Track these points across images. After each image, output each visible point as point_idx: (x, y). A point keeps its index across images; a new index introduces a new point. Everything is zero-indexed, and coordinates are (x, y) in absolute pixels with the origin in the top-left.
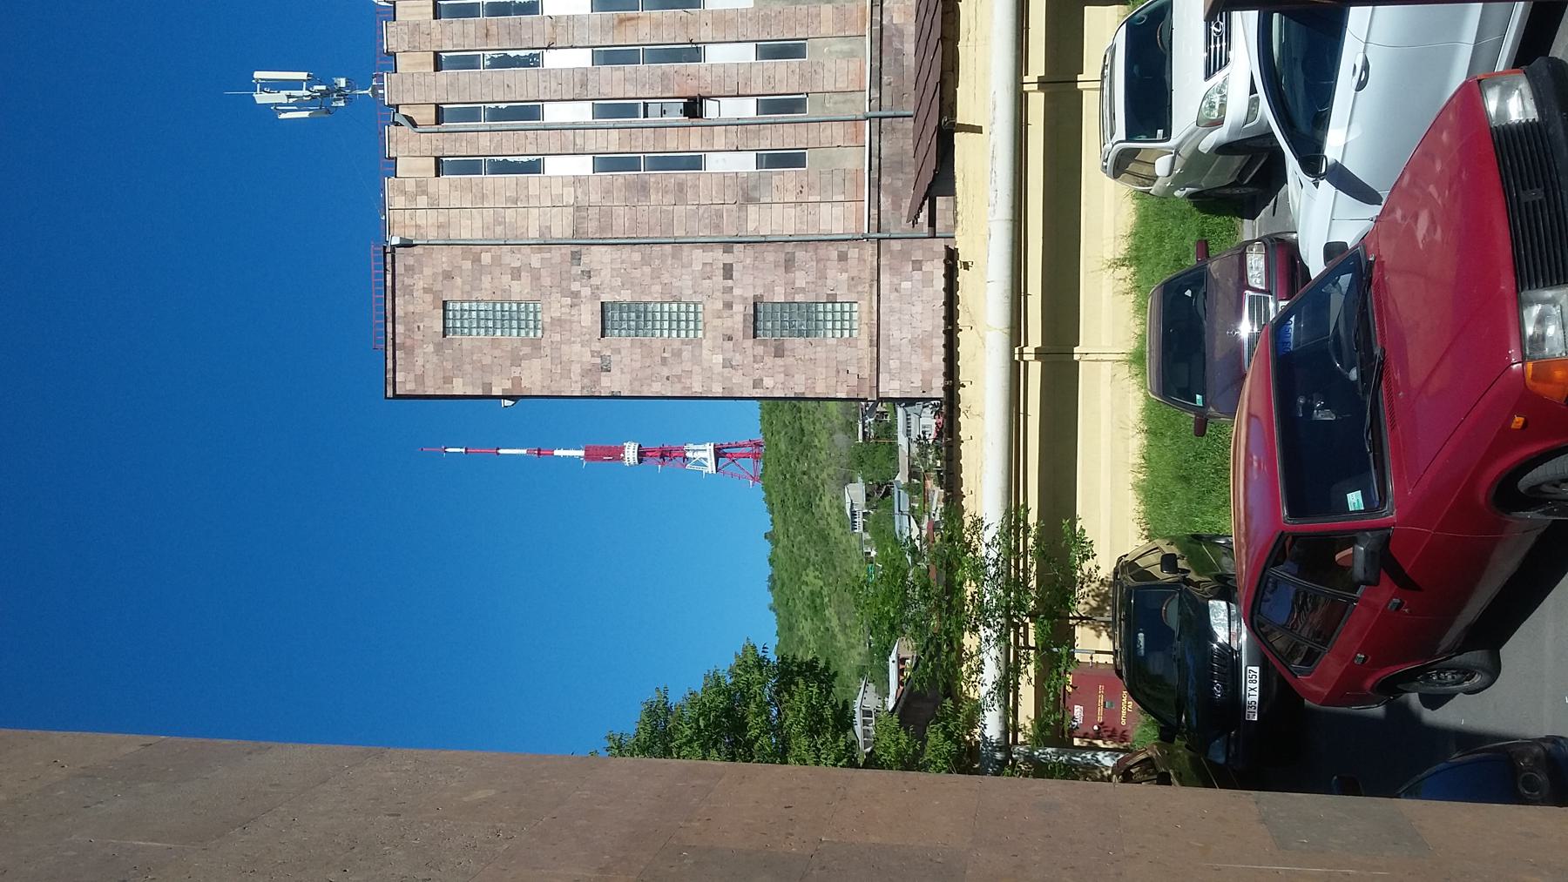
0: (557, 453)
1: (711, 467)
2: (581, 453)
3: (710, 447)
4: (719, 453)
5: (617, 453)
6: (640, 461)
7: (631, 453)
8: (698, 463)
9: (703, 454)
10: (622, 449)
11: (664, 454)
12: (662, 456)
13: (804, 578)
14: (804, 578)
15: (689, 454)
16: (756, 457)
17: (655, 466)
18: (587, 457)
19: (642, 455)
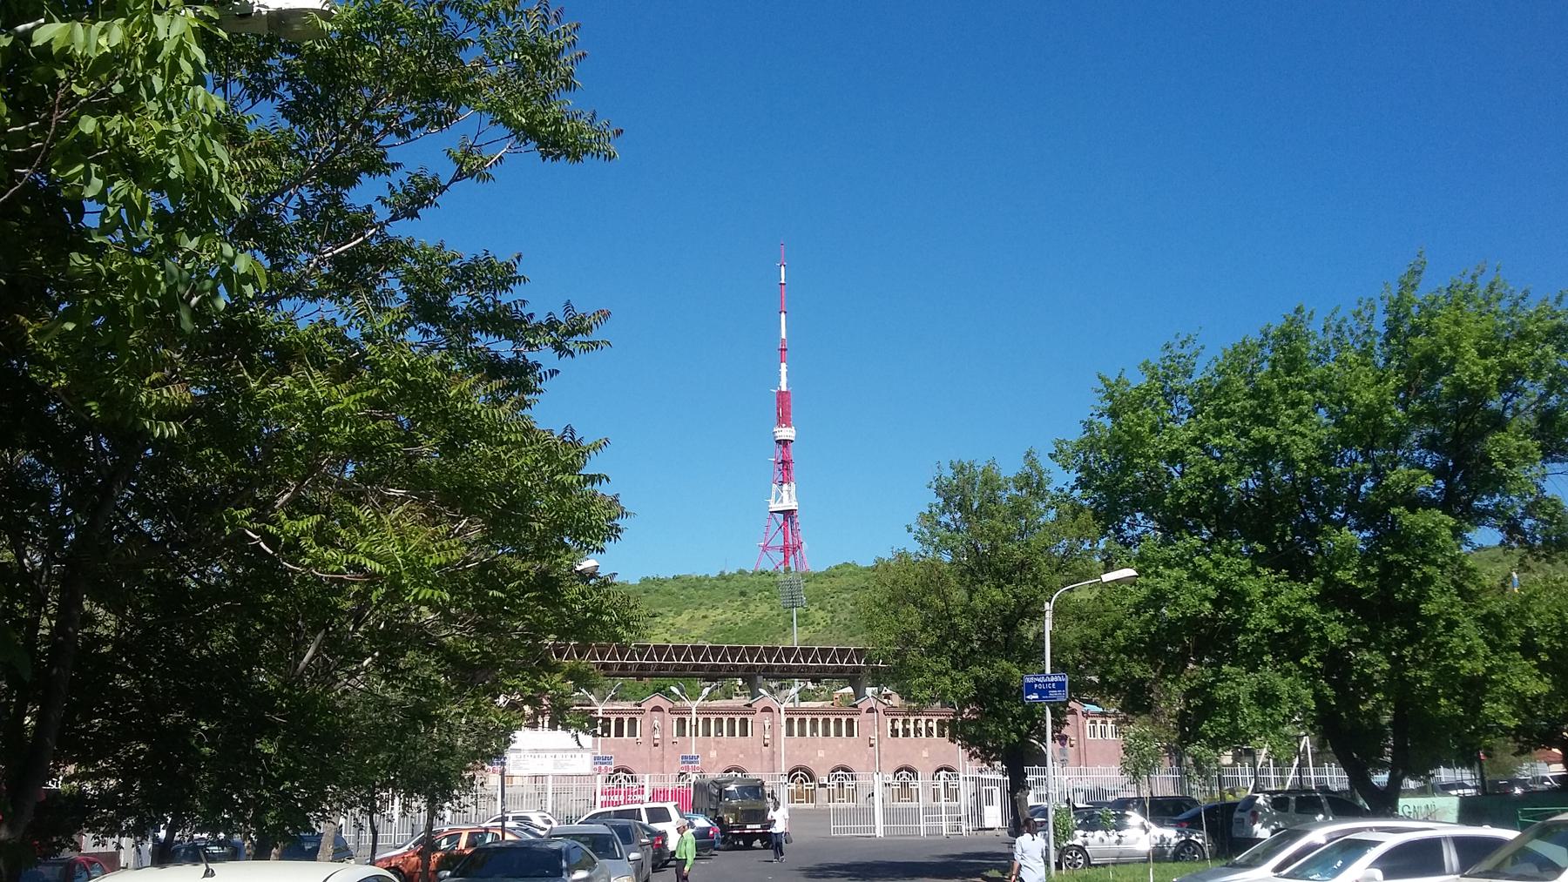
0: (784, 365)
1: (775, 507)
2: (784, 389)
3: (793, 505)
4: (788, 514)
5: (784, 420)
6: (779, 442)
7: (786, 433)
8: (778, 495)
9: (789, 503)
10: (788, 425)
11: (785, 464)
12: (783, 462)
13: (812, 609)
14: (812, 609)
15: (785, 486)
16: (785, 549)
17: (773, 455)
18: (780, 392)
19: (784, 443)
